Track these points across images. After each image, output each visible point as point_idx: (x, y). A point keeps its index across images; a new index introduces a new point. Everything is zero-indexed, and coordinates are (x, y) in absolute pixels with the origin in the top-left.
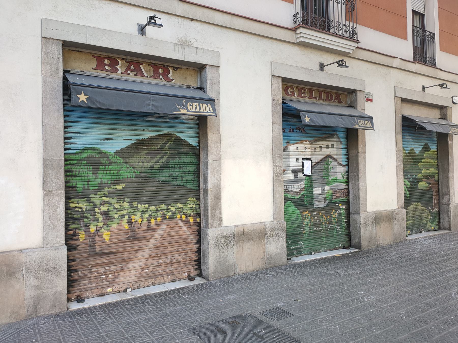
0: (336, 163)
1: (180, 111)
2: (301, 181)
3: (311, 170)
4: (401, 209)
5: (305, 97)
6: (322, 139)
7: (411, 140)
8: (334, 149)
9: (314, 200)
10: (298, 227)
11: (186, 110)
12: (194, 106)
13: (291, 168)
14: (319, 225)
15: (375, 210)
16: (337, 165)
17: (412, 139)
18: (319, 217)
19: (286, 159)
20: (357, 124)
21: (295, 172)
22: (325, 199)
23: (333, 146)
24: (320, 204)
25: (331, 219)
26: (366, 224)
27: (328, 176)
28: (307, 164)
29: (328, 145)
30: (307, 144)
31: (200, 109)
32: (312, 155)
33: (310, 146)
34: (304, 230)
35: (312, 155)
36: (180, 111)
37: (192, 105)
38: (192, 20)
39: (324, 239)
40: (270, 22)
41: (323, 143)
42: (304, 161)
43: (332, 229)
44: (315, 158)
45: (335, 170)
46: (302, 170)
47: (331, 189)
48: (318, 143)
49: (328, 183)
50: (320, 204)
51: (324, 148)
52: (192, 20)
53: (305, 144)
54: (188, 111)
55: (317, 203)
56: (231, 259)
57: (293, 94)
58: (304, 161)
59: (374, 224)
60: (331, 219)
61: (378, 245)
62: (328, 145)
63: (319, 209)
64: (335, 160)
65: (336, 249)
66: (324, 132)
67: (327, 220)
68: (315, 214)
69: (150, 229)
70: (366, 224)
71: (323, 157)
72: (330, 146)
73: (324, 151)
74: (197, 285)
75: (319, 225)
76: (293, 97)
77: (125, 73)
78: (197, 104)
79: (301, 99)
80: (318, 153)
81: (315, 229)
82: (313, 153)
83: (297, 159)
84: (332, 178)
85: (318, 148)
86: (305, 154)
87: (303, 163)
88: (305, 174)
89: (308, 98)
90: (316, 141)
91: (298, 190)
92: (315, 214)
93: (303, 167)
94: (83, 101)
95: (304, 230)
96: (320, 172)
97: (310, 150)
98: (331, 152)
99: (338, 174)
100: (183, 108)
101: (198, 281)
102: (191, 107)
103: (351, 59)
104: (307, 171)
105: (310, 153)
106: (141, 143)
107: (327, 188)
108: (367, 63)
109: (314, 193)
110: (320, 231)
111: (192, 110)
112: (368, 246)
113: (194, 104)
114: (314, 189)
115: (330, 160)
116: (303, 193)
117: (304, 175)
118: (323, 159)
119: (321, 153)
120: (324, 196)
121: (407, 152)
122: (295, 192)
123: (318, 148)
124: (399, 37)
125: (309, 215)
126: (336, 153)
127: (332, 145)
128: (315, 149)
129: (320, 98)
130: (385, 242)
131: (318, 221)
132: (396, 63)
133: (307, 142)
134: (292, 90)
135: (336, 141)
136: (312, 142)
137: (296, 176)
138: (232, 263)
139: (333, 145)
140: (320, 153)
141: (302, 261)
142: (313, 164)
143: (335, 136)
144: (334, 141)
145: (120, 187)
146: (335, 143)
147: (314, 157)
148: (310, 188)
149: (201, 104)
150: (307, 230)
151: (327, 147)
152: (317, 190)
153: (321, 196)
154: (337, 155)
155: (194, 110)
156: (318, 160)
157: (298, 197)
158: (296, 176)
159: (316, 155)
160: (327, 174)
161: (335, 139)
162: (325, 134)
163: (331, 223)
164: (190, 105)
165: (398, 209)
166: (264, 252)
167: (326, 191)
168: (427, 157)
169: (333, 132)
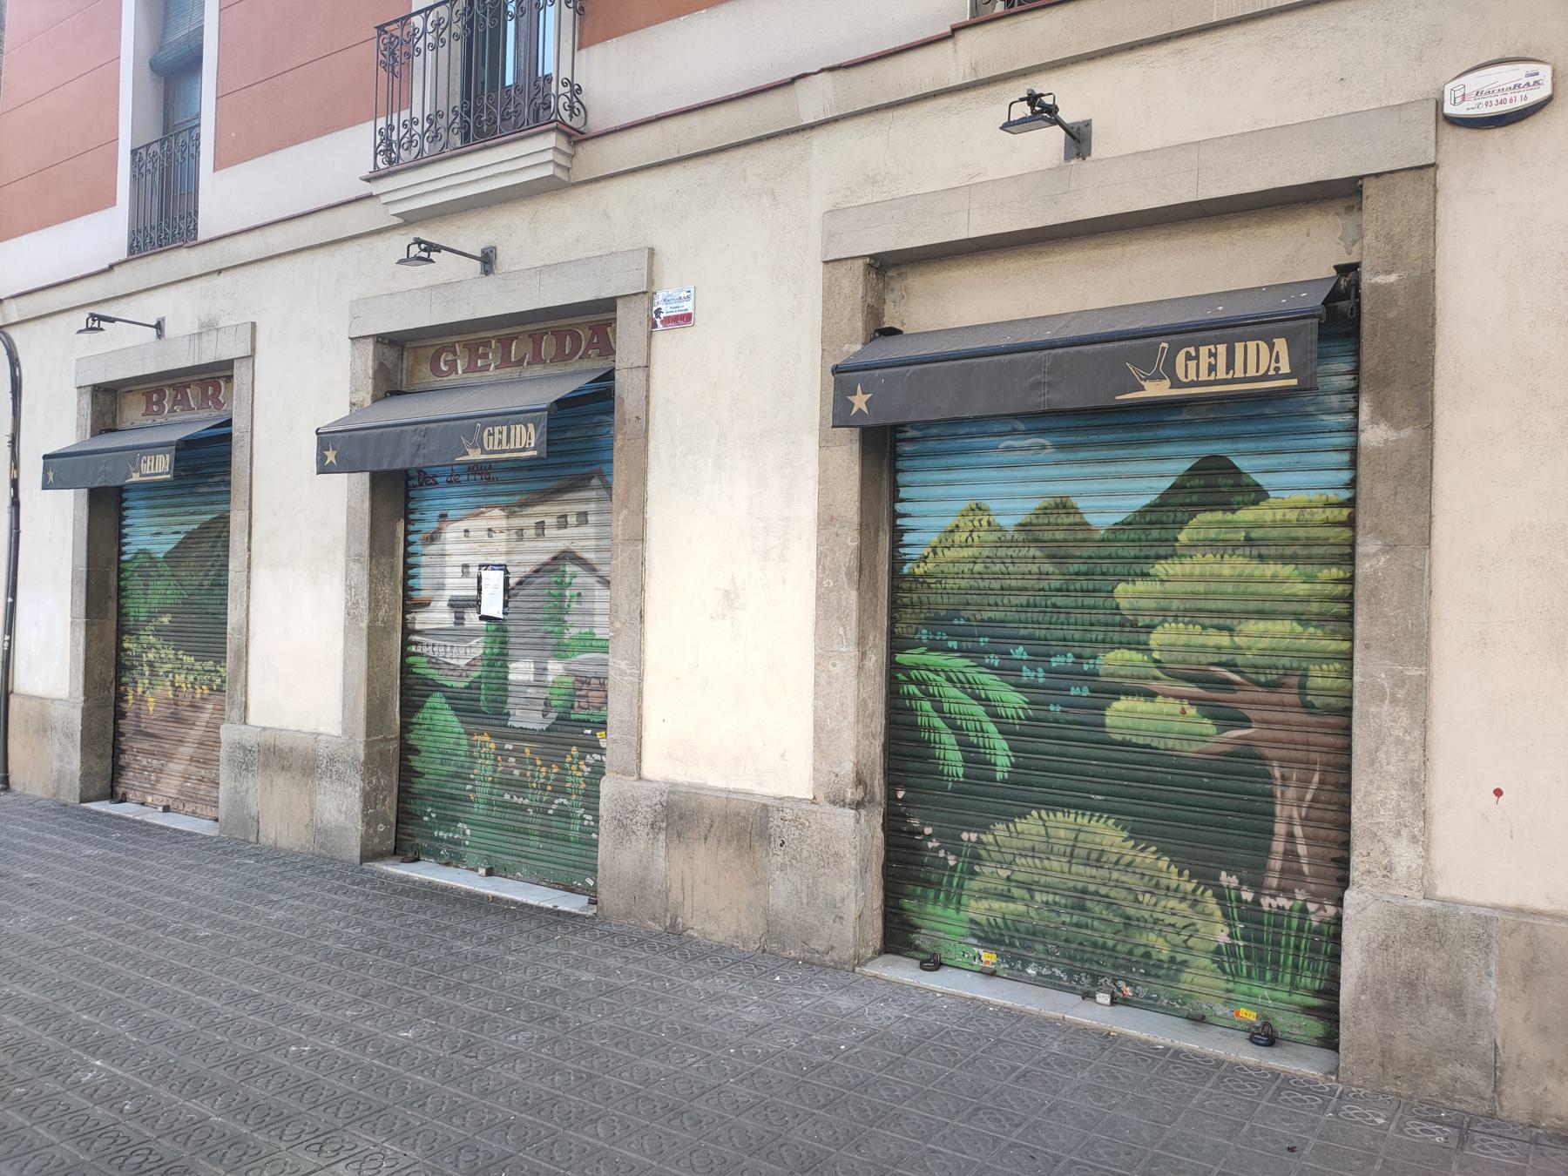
0: (592, 580)
1: (1142, 389)
2: (473, 633)
3: (506, 604)
4: (829, 808)
5: (486, 368)
6: (545, 496)
7: (1049, 455)
8: (589, 530)
9: (510, 700)
10: (456, 775)
11: (1167, 382)
12: (1204, 361)
13: (448, 594)
14: (521, 786)
15: (679, 779)
16: (598, 586)
17: (1060, 447)
18: (520, 761)
19: (434, 566)
20: (139, 470)
21: (459, 606)
22: (547, 703)
23: (583, 518)
24: (527, 718)
25: (561, 779)
26: (621, 825)
27: (561, 622)
28: (494, 580)
29: (565, 516)
30: (496, 518)
31: (1230, 366)
32: (508, 553)
33: (503, 523)
34: (473, 791)
35: (508, 553)
36: (1142, 389)
37: (1197, 357)
38: (219, 272)
39: (535, 841)
40: (323, 205)
41: (547, 512)
42: (485, 574)
43: (564, 814)
44: (519, 564)
45: (587, 606)
46: (476, 603)
47: (569, 673)
48: (530, 510)
49: (560, 651)
50: (527, 718)
51: (551, 527)
52: (219, 272)
53: (492, 518)
54: (1176, 383)
55: (518, 712)
56: (254, 803)
57: (453, 367)
58: (485, 574)
59: (662, 837)
60: (561, 779)
61: (674, 925)
62: (565, 516)
63: (524, 735)
64: (583, 563)
65: (572, 891)
66: (556, 472)
67: (547, 778)
68: (509, 746)
69: (194, 707)
70: (621, 825)
71: (546, 558)
72: (572, 520)
73: (551, 539)
74: (1282, 1081)
75: (521, 786)
76: (453, 376)
77: (172, 411)
78: (1222, 349)
79: (475, 377)
80: (527, 545)
81: (507, 797)
82: (513, 544)
83: (466, 566)
84: (574, 631)
85: (528, 528)
86: (489, 548)
87: (479, 579)
88: (483, 613)
89: (497, 368)
90: (524, 505)
91: (462, 663)
92: (509, 746)
93: (480, 590)
94: (853, 404)
95: (473, 791)
96: (534, 611)
97: (504, 536)
98: (573, 540)
99: (596, 618)
100: (1158, 377)
101: (1304, 1065)
102: (1192, 364)
103: (595, 186)
104: (493, 604)
105: (503, 548)
106: (190, 536)
107: (555, 668)
108: (678, 168)
109: (511, 677)
110: (523, 808)
111: (1192, 377)
112: (628, 914)
113: (1204, 350)
114: (512, 666)
115: (570, 568)
116: (476, 674)
117: (482, 618)
118: (546, 564)
119: (540, 544)
120: (543, 693)
121: (1009, 522)
122: (456, 668)
123: (528, 528)
124: (689, 13)
125: (492, 746)
126: (593, 543)
127: (579, 514)
128: (520, 532)
129: (537, 359)
130: (711, 927)
131: (517, 772)
132: (812, 101)
133: (497, 512)
134: (450, 357)
135: (598, 500)
136: (511, 511)
137: (459, 619)
138: (253, 813)
139: (586, 514)
140: (534, 544)
141: (1132, 1032)
142: (512, 582)
143: (595, 482)
144: (588, 500)
145: (166, 620)
146: (592, 507)
147: (516, 558)
148: (498, 660)
149: (1239, 347)
150: (483, 792)
151: (563, 522)
152: (520, 671)
153: (531, 690)
154: (598, 550)
155: (1204, 376)
156: (528, 569)
157: (462, 685)
158: (459, 619)
159: (522, 553)
160: (558, 616)
161: (593, 494)
162: (556, 477)
163: (560, 791)
164: (1188, 357)
165: (814, 801)
166: (312, 811)
167: (550, 678)
168: (1193, 545)
169: (587, 469)
